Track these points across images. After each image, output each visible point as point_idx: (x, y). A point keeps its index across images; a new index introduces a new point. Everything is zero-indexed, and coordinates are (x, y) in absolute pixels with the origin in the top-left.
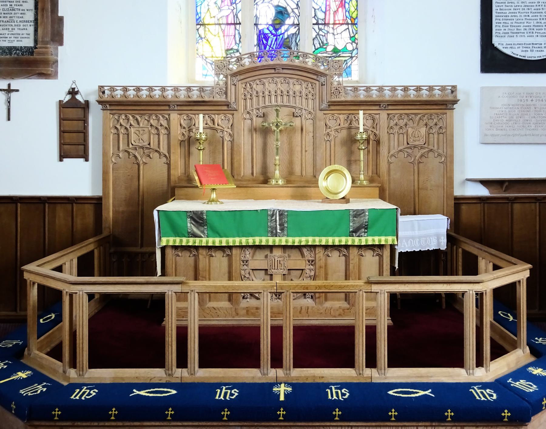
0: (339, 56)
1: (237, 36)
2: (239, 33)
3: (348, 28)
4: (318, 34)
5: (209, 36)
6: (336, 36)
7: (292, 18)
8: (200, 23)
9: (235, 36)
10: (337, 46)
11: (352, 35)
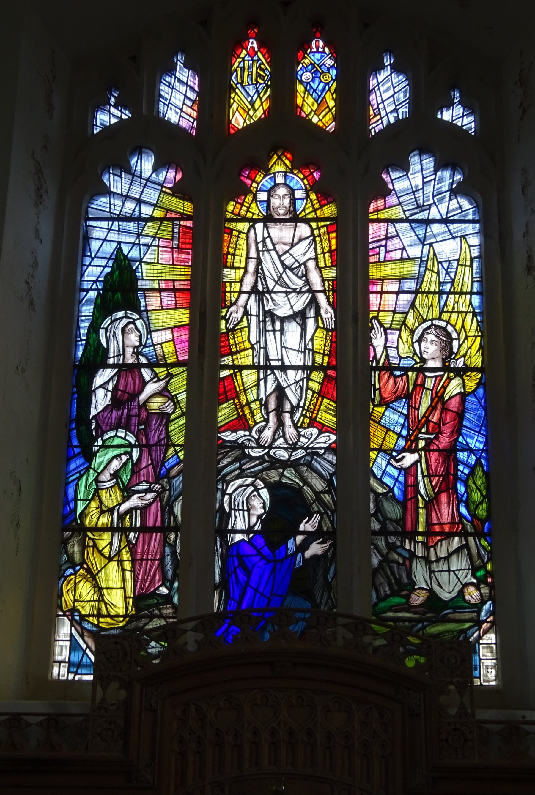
0: (446, 620)
1: (168, 559)
2: (174, 553)
3: (467, 546)
4: (386, 560)
5: (95, 561)
6: (434, 567)
7: (317, 517)
9: (162, 560)
10: (436, 588)
11: (478, 562)
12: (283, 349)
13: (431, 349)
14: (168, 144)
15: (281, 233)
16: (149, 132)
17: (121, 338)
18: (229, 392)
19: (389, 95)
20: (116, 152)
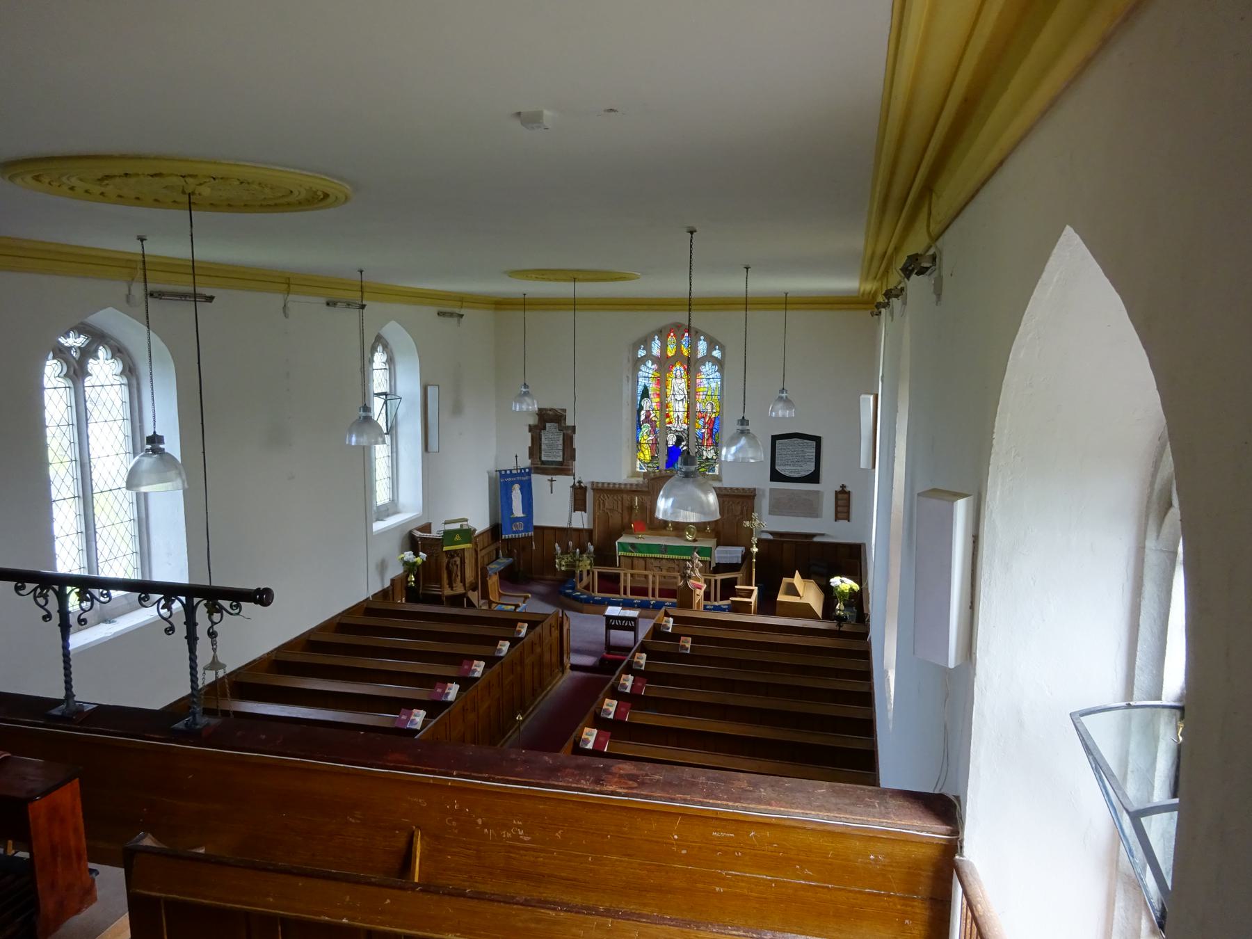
8: (639, 443)
12: (678, 408)
13: (709, 408)
14: (656, 360)
15: (679, 381)
16: (649, 356)
17: (646, 404)
18: (668, 416)
19: (702, 347)
20: (643, 361)
